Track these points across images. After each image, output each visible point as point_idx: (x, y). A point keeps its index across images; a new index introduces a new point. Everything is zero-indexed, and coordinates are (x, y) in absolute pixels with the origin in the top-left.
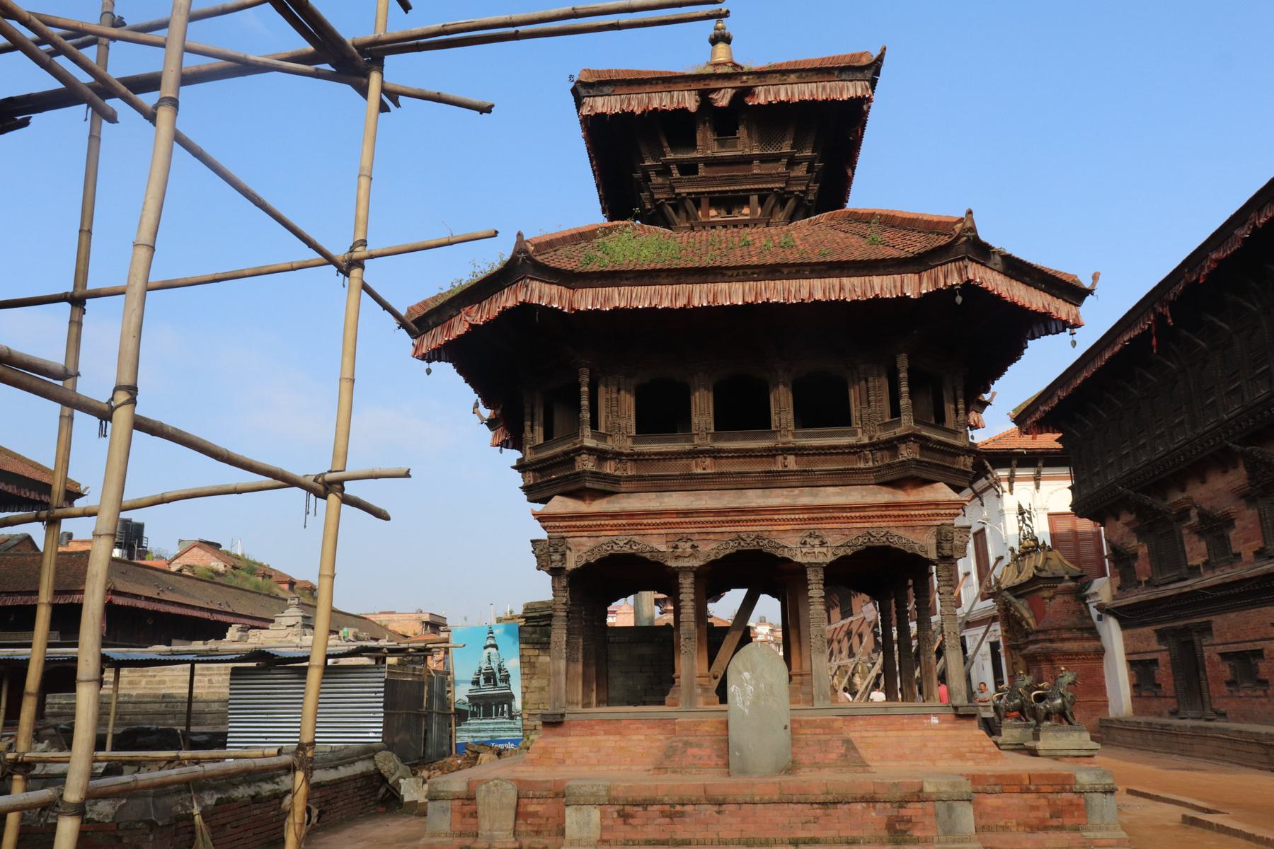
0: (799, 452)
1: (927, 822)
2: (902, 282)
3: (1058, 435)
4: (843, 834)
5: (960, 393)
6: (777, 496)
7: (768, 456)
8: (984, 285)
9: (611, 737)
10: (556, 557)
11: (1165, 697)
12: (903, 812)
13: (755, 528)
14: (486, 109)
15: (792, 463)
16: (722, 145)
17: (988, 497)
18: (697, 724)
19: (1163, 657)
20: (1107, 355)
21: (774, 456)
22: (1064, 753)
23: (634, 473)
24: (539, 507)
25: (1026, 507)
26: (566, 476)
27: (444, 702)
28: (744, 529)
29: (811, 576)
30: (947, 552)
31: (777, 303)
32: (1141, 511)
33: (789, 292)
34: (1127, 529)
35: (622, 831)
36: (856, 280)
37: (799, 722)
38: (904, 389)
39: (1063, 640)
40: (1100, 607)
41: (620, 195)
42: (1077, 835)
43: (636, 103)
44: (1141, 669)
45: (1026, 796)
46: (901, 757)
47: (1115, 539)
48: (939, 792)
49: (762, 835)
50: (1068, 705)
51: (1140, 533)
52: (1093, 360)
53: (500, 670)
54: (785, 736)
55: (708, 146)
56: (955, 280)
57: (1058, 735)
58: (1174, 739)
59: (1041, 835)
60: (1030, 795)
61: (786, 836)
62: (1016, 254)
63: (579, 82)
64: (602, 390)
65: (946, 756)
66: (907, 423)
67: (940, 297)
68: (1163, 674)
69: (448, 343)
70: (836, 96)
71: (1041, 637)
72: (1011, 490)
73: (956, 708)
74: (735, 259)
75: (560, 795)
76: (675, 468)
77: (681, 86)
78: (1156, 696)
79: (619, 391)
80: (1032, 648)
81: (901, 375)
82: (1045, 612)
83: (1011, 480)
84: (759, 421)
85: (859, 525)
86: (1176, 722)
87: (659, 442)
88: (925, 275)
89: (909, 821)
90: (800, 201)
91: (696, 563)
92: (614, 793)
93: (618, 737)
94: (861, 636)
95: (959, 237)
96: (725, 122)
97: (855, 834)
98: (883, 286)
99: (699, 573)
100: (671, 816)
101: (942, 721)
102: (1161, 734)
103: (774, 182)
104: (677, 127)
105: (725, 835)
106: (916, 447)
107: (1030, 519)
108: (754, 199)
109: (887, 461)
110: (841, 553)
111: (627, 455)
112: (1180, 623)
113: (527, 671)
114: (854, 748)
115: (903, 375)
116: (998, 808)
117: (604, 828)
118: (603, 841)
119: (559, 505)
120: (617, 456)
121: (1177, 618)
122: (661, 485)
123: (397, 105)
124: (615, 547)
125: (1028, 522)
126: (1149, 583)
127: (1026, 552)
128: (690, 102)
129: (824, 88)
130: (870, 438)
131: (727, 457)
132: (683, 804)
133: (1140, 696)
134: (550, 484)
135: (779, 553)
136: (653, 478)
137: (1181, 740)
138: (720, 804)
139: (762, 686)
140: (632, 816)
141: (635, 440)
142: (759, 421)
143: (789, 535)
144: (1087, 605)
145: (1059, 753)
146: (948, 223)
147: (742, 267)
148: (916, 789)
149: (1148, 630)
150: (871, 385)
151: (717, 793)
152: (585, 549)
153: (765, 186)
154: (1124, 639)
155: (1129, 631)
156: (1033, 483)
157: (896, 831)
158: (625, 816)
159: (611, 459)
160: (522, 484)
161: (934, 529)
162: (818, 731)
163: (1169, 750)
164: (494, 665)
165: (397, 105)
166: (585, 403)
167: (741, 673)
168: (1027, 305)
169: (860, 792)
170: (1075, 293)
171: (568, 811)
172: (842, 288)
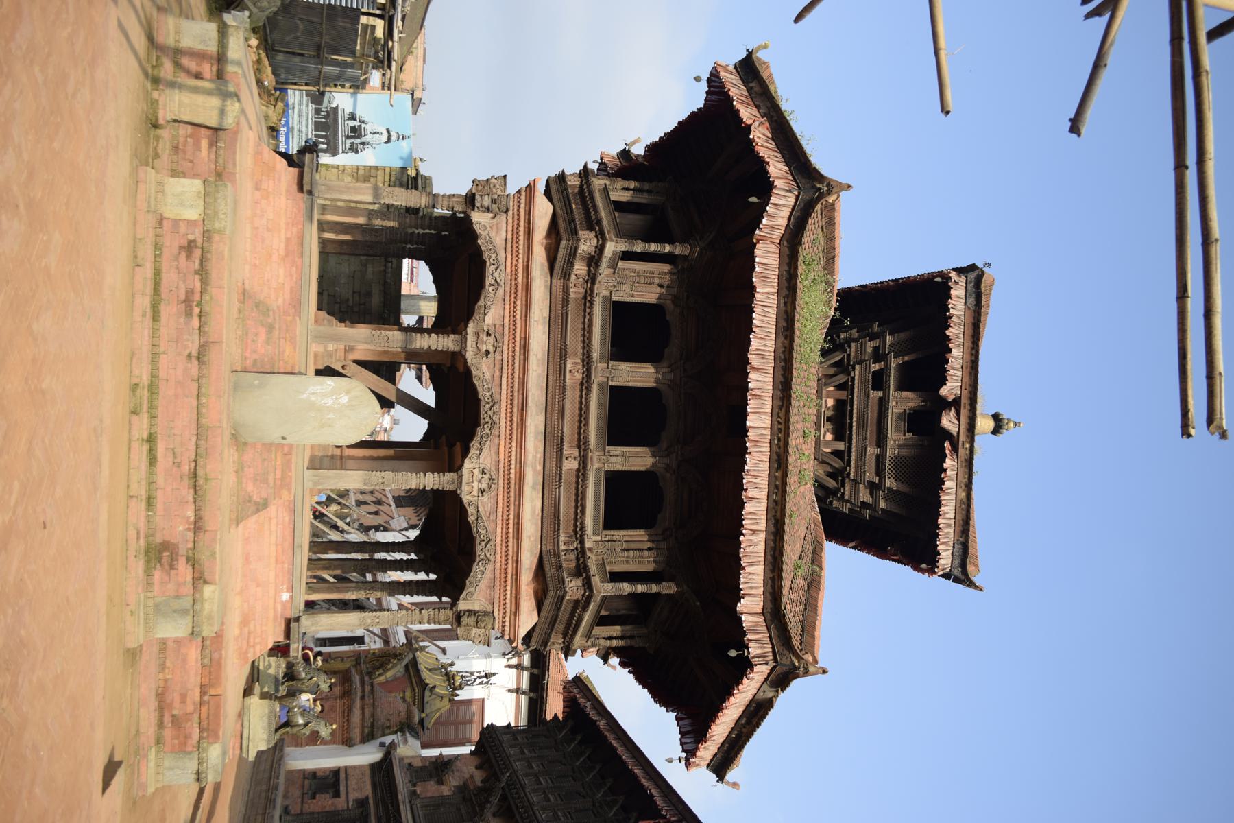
0: (581, 473)
1: (171, 586)
2: (755, 595)
3: (561, 717)
4: (159, 494)
5: (629, 642)
6: (536, 447)
7: (579, 440)
8: (745, 681)
9: (283, 245)
10: (486, 201)
11: (302, 802)
12: (182, 561)
13: (503, 421)
14: (1075, 126)
15: (570, 465)
16: (900, 416)
18: (293, 341)
19: (340, 804)
20: (638, 771)
21: (579, 447)
22: (246, 723)
23: (572, 295)
24: (541, 187)
25: (493, 680)
26: (573, 220)
27: (336, 82)
28: (503, 409)
29: (449, 477)
30: (464, 620)
31: (745, 462)
32: (485, 791)
33: (756, 477)
34: (467, 776)
35: (171, 244)
36: (761, 547)
37: (290, 453)
38: (640, 588)
39: (363, 709)
40: (393, 745)
41: (863, 307)
42: (152, 740)
43: (956, 332)
44: (330, 781)
45: (197, 691)
46: (247, 559)
47: (458, 763)
48: (203, 601)
49: (161, 403)
50: (295, 730)
51: (462, 789)
52: (634, 757)
53: (363, 144)
54: (274, 436)
55: (901, 402)
56: (754, 650)
57: (265, 719)
58: (260, 811)
59: (153, 704)
60: (198, 694)
61: (158, 430)
62: (772, 713)
63: (983, 273)
64: (666, 268)
65: (246, 606)
66: (604, 589)
67: (737, 635)
68: (325, 802)
69: (729, 100)
70: (942, 538)
71: (367, 688)
72: (509, 666)
73: (297, 619)
74: (796, 422)
75: (219, 176)
76: (574, 340)
77: (966, 379)
79: (661, 286)
80: (356, 679)
81: (654, 586)
82: (390, 692)
83: (519, 667)
84: (617, 434)
85: (499, 531)
86: (277, 812)
87: (603, 326)
88: (761, 619)
89: (172, 567)
90: (833, 492)
91: (470, 355)
92: (216, 238)
93: (282, 253)
94: (376, 513)
95: (799, 658)
96: (924, 423)
97: (159, 506)
98: (753, 576)
99: (457, 357)
100: (187, 301)
101: (284, 604)
102: (266, 798)
103: (856, 467)
104: (925, 372)
105: (163, 361)
106: (578, 595)
107: (481, 683)
108: (841, 446)
109: (565, 565)
110: (471, 510)
111: (591, 289)
113: (361, 172)
114: (258, 511)
115: (654, 588)
116: (184, 661)
117: (176, 222)
118: (161, 220)
119: (543, 210)
120: (592, 278)
122: (558, 323)
123: (1089, 15)
124: (492, 268)
125: (478, 681)
127: (449, 677)
128: (952, 387)
129: (949, 526)
130: (590, 549)
131: (581, 397)
132: (200, 316)
134: (567, 202)
135: (474, 444)
136: (565, 315)
138: (198, 358)
139: (331, 416)
140: (188, 257)
141: (606, 300)
142: (617, 434)
143: (494, 456)
144: (396, 732)
145: (246, 719)
146: (813, 646)
147: (787, 428)
148: (207, 576)
149: (368, 791)
150: (646, 553)
151: (212, 355)
152: (493, 234)
153: (853, 458)
155: (368, 772)
157: (160, 552)
158: (189, 247)
159: (589, 271)
160: (567, 172)
161: (489, 609)
162: (279, 473)
164: (368, 138)
165: (1089, 15)
166: (652, 247)
167: (347, 392)
168: (717, 721)
169: (206, 514)
170: (721, 766)
171: (197, 183)
172: (754, 532)
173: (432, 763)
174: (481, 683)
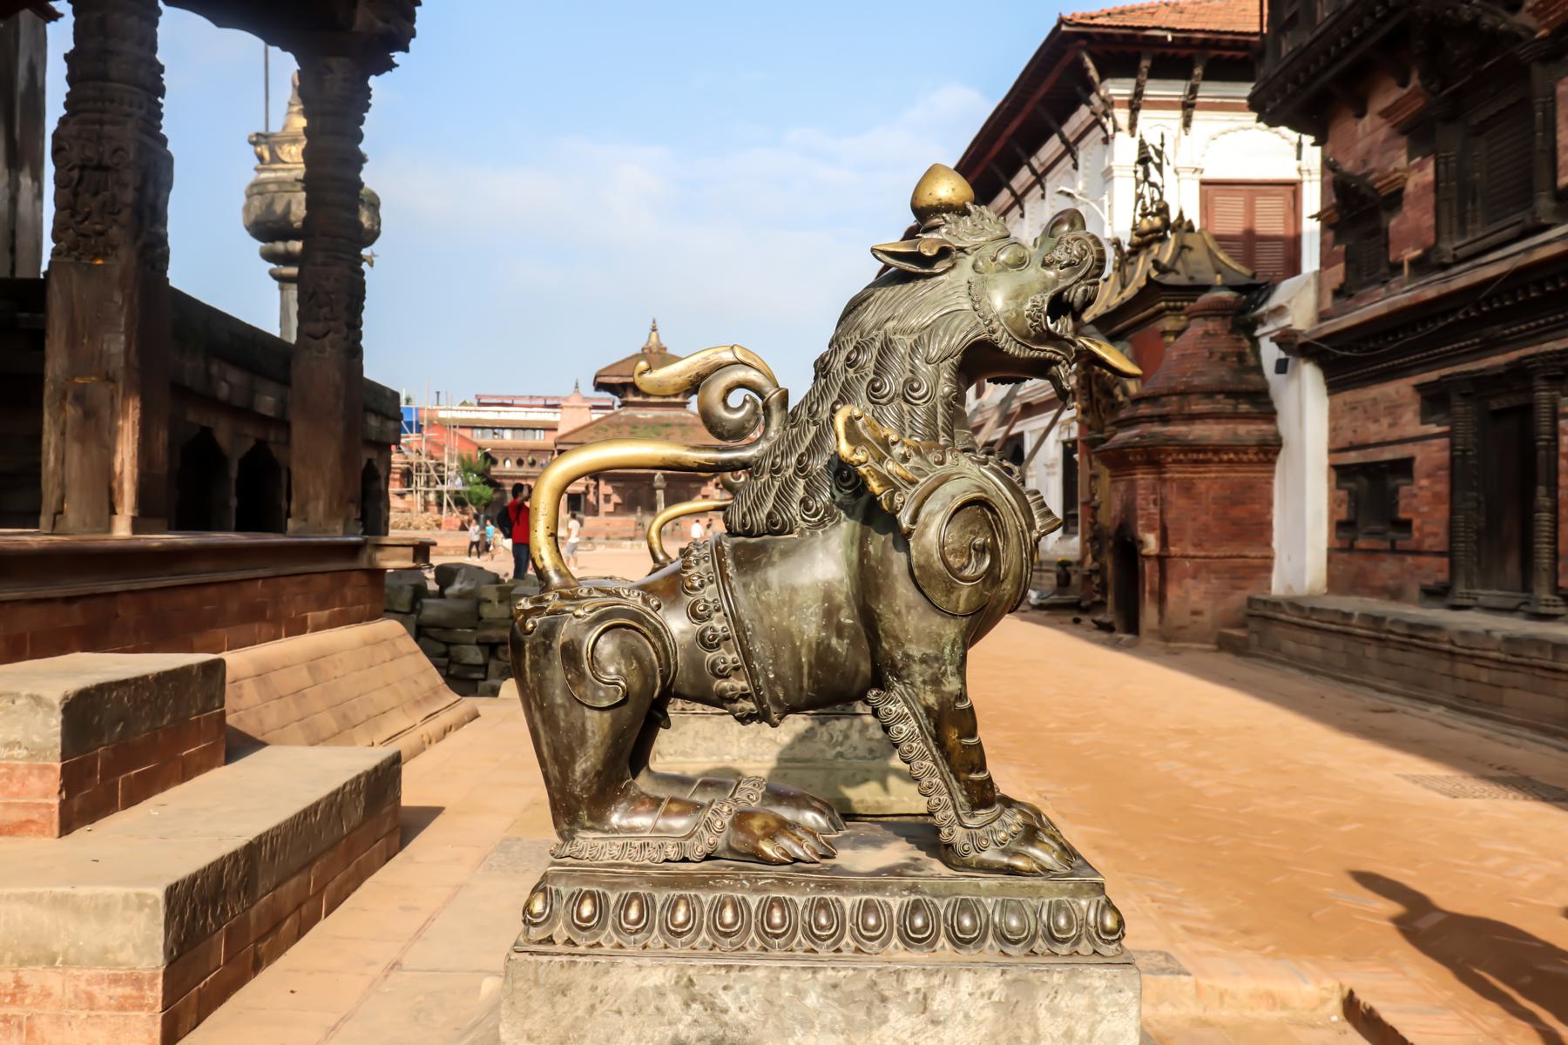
11: (1417, 552)
17: (1088, 151)
19: (1431, 455)
39: (1192, 418)
40: (1286, 340)
44: (1367, 489)
47: (1348, 165)
51: (1417, 132)
58: (1443, 665)
71: (1144, 410)
72: (1133, 125)
78: (1393, 550)
80: (1123, 436)
83: (1135, 105)
86: (1436, 614)
102: (1404, 647)
107: (1159, 167)
112: (1499, 360)
121: (1493, 345)
125: (1154, 176)
126: (1422, 266)
127: (1145, 240)
133: (1350, 549)
137: (1464, 669)
144: (1255, 342)
149: (1401, 389)
154: (1334, 415)
155: (1349, 396)
156: (1177, 115)
163: (1420, 690)
173: (1337, 240)
174: (1159, 167)
